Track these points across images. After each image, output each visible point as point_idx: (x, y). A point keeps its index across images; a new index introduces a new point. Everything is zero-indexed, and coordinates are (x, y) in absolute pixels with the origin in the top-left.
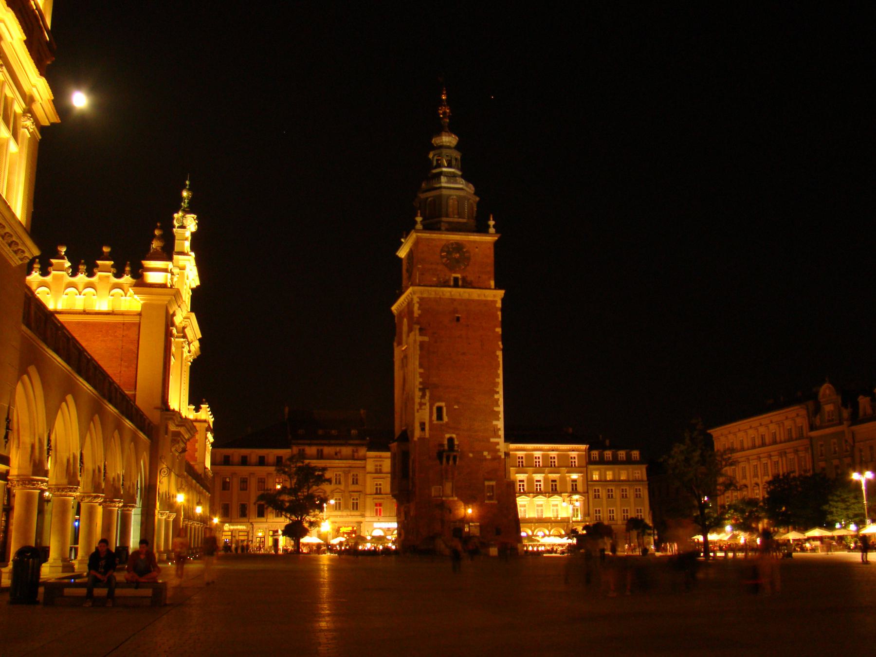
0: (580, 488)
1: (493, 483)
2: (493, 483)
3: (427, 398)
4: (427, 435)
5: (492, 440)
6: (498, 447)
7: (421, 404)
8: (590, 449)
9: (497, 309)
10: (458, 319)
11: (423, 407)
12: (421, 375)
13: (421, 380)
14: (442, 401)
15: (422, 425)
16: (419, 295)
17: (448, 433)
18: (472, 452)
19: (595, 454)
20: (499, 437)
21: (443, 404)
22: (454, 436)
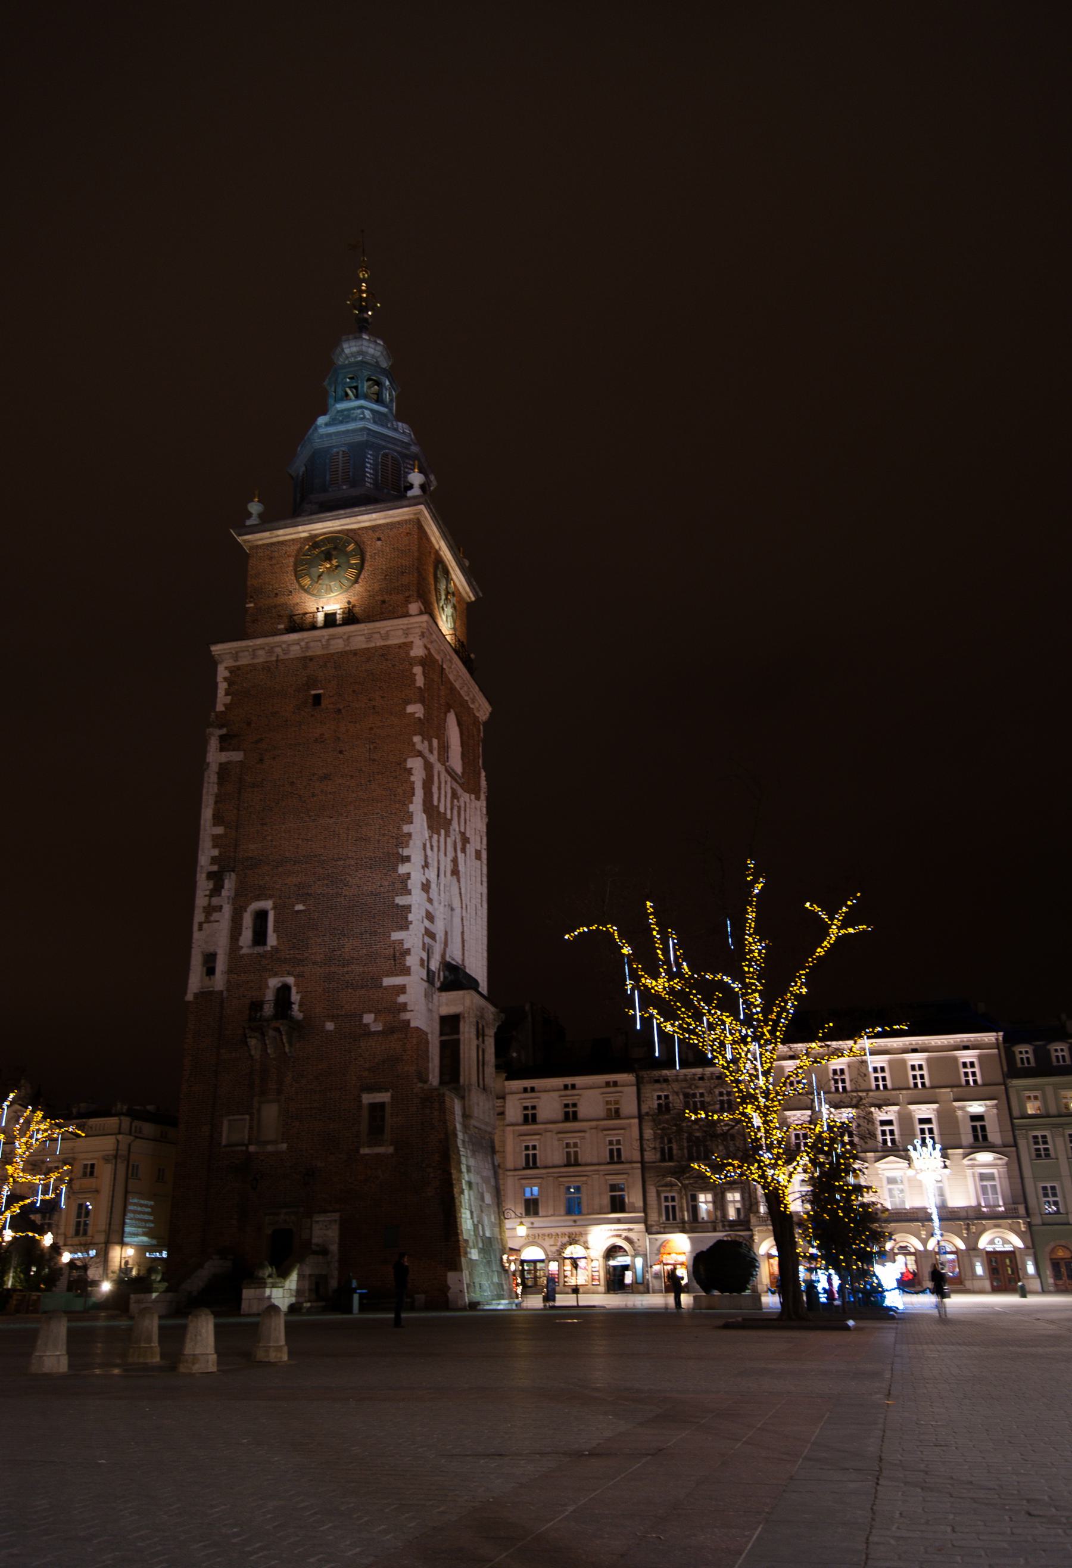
0: (994, 1137)
1: (384, 1097)
2: (384, 1097)
3: (224, 893)
4: (219, 982)
5: (388, 981)
6: (402, 999)
7: (210, 910)
8: (1010, 1041)
9: (413, 662)
10: (317, 699)
11: (215, 916)
12: (216, 841)
13: (216, 852)
14: (271, 897)
15: (210, 959)
16: (230, 663)
17: (275, 975)
18: (332, 1018)
19: (1024, 1052)
20: (406, 971)
21: (268, 904)
22: (290, 980)
